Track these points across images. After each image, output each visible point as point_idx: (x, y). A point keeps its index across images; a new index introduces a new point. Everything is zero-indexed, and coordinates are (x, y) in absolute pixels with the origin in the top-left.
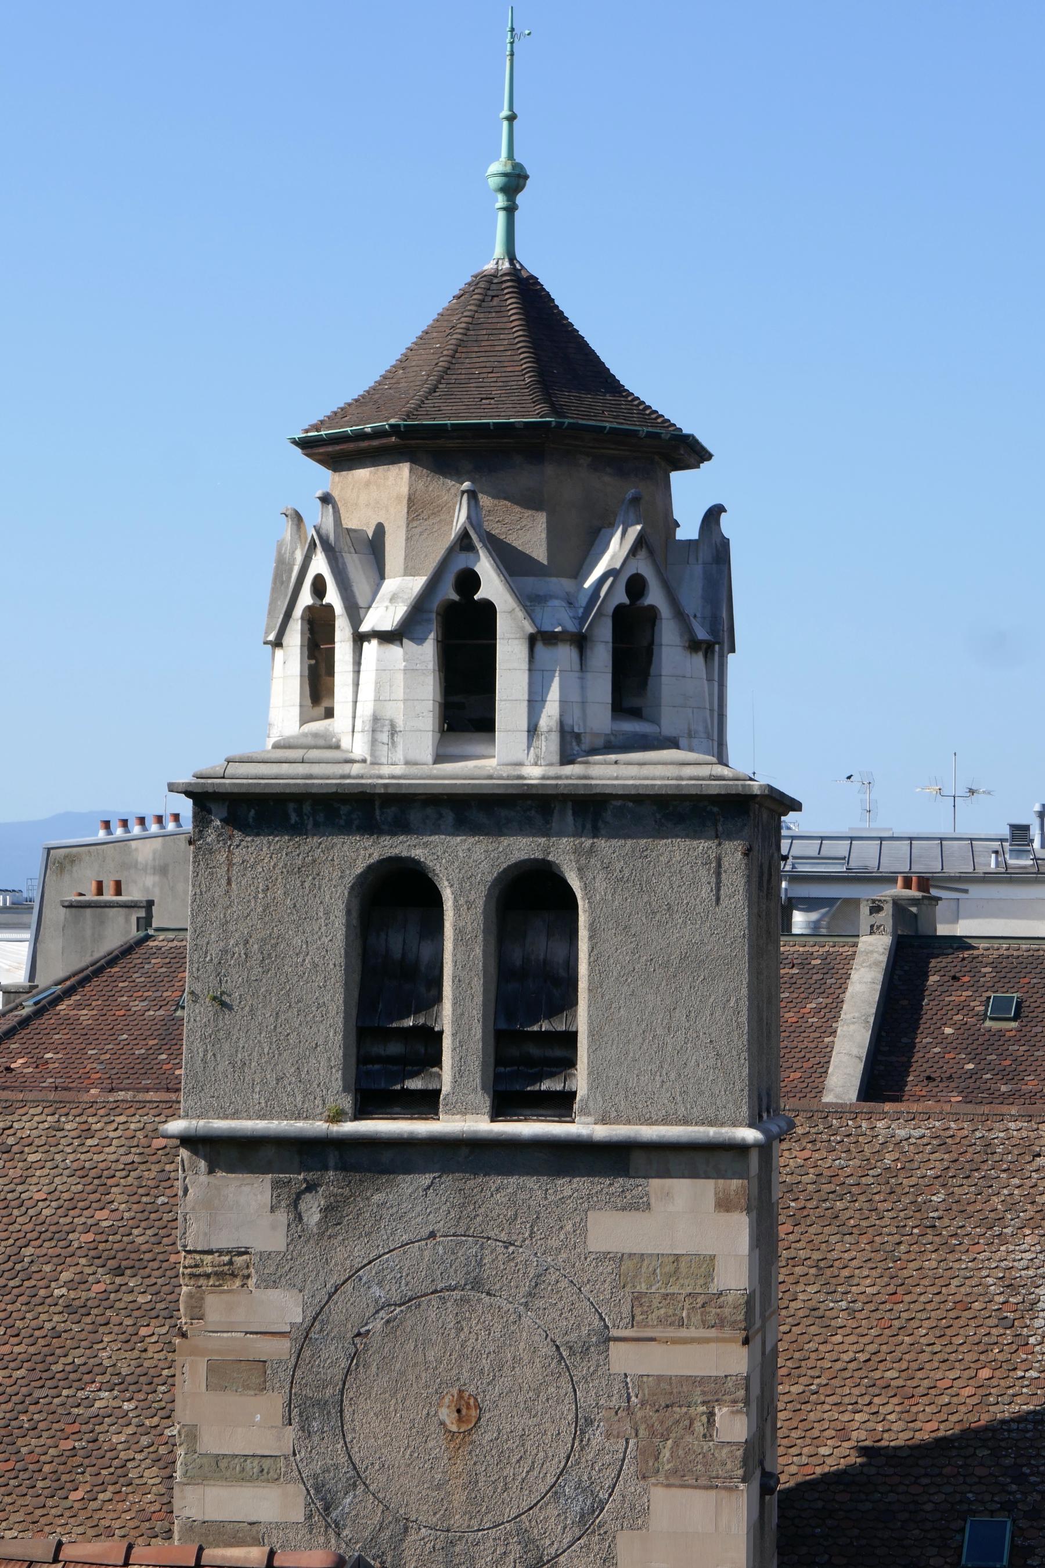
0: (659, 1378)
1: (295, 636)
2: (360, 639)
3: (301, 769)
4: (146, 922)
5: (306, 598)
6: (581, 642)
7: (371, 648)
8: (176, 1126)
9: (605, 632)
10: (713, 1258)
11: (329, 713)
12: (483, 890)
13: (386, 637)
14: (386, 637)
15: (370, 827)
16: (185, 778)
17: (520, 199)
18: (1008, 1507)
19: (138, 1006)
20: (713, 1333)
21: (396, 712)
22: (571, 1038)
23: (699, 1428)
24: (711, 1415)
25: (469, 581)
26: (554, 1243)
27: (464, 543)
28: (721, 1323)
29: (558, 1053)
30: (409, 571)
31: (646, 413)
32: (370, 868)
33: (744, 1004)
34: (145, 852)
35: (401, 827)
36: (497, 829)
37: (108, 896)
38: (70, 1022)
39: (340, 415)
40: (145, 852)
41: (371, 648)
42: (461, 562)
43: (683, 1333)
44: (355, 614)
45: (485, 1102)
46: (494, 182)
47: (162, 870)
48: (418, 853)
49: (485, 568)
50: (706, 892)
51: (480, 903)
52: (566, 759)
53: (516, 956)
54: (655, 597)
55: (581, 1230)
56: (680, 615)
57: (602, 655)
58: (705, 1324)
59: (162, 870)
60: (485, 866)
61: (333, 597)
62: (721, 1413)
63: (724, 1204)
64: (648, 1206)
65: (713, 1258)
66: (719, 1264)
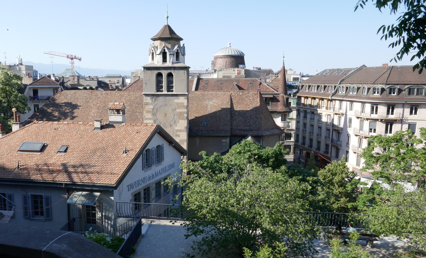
1: (151, 54)
2: (156, 55)
3: (152, 65)
4: (139, 78)
5: (152, 52)
6: (173, 55)
7: (157, 55)
8: (143, 93)
9: (175, 54)
11: (154, 61)
13: (158, 55)
14: (158, 55)
15: (157, 70)
16: (143, 66)
18: (206, 121)
19: (139, 84)
21: (159, 61)
22: (173, 86)
25: (164, 50)
27: (164, 47)
28: (185, 107)
29: (172, 87)
30: (160, 49)
31: (178, 36)
34: (139, 72)
35: (160, 70)
36: (167, 70)
37: (136, 76)
38: (134, 86)
39: (154, 37)
40: (139, 72)
41: (157, 55)
42: (164, 48)
44: (156, 53)
45: (167, 91)
47: (140, 74)
48: (161, 72)
49: (166, 49)
50: (183, 74)
52: (172, 64)
53: (169, 80)
54: (179, 51)
56: (181, 52)
57: (175, 56)
59: (140, 74)
61: (154, 51)
63: (185, 99)
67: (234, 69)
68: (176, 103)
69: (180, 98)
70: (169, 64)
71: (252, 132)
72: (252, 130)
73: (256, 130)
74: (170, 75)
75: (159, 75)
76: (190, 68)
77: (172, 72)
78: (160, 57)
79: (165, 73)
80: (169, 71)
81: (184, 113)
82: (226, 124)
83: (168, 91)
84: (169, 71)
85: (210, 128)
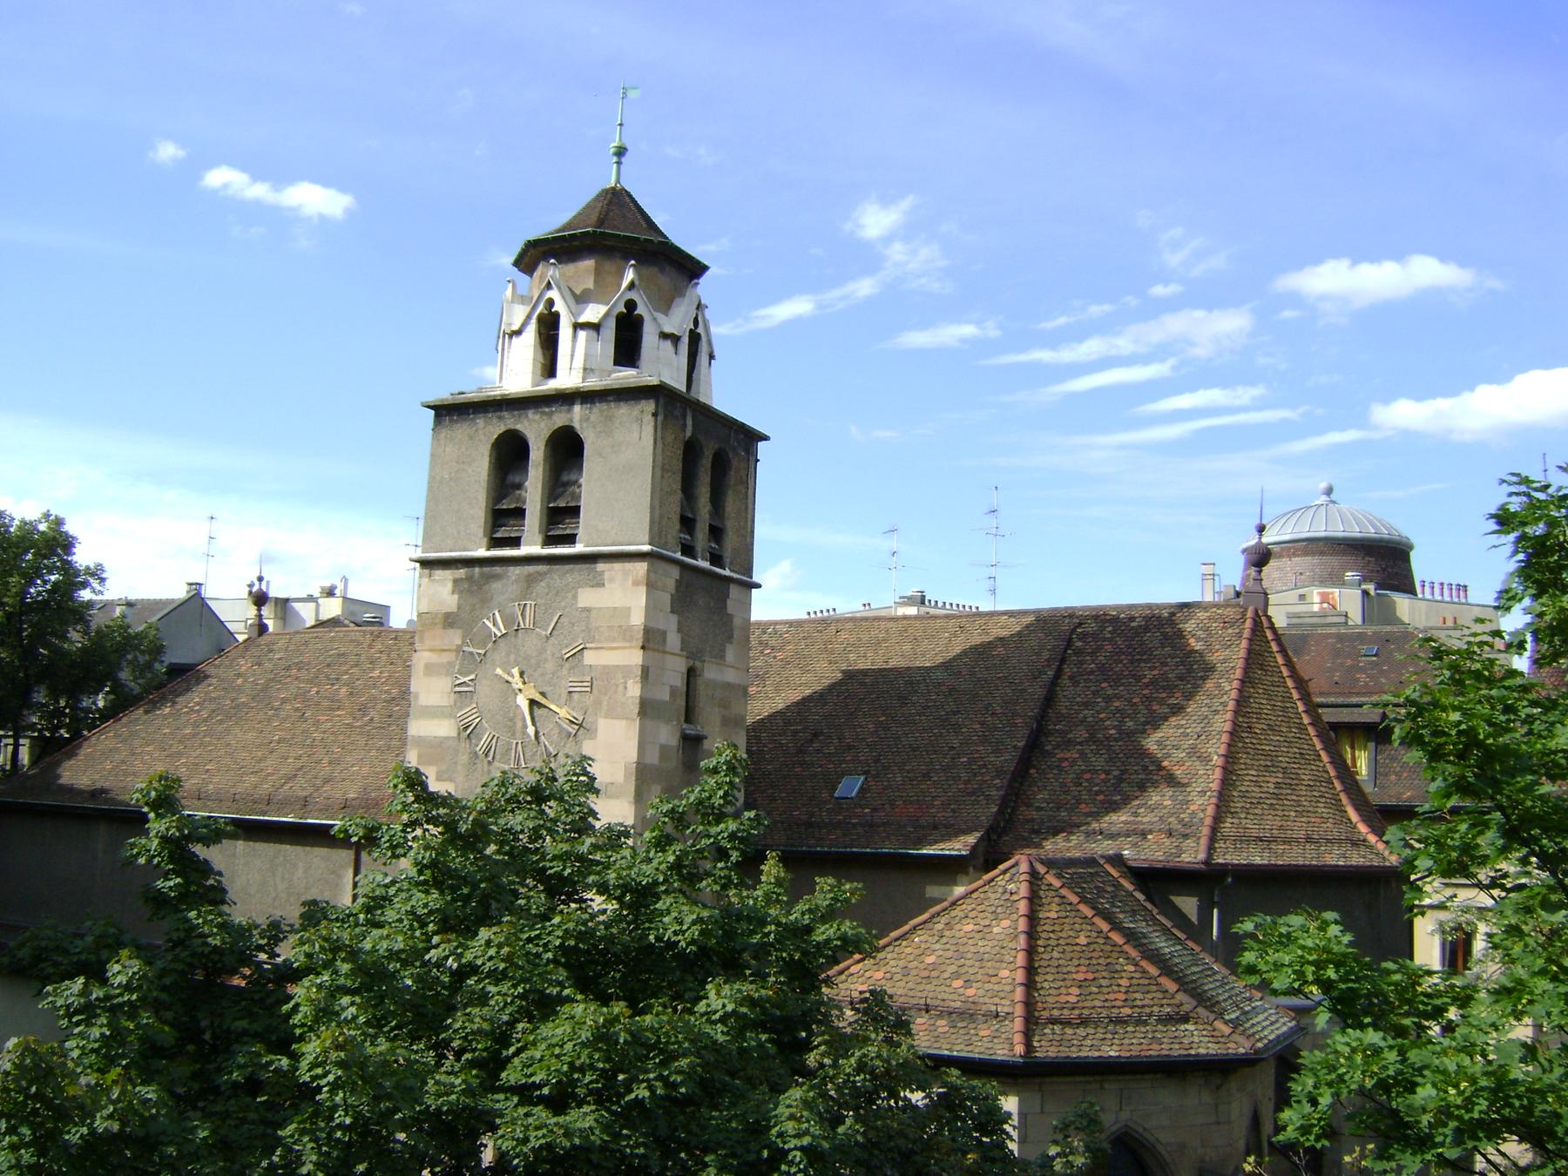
0: (605, 667)
10: (630, 608)
12: (544, 443)
17: (623, 160)
20: (627, 645)
23: (621, 688)
24: (626, 683)
26: (563, 604)
28: (631, 639)
32: (500, 435)
33: (650, 486)
43: (615, 645)
45: (539, 538)
46: (612, 150)
48: (519, 427)
50: (636, 435)
51: (543, 448)
52: (584, 380)
55: (575, 597)
58: (624, 639)
60: (545, 431)
62: (630, 682)
64: (604, 585)
65: (630, 608)
66: (633, 609)
67: (1301, 591)
68: (587, 610)
69: (612, 580)
70: (568, 377)
71: (1135, 845)
72: (1144, 834)
73: (1170, 834)
74: (567, 448)
75: (511, 452)
76: (765, 438)
77: (577, 415)
78: (526, 347)
79: (536, 430)
80: (559, 419)
81: (625, 671)
82: (973, 793)
83: (550, 540)
84: (559, 419)
85: (875, 810)
